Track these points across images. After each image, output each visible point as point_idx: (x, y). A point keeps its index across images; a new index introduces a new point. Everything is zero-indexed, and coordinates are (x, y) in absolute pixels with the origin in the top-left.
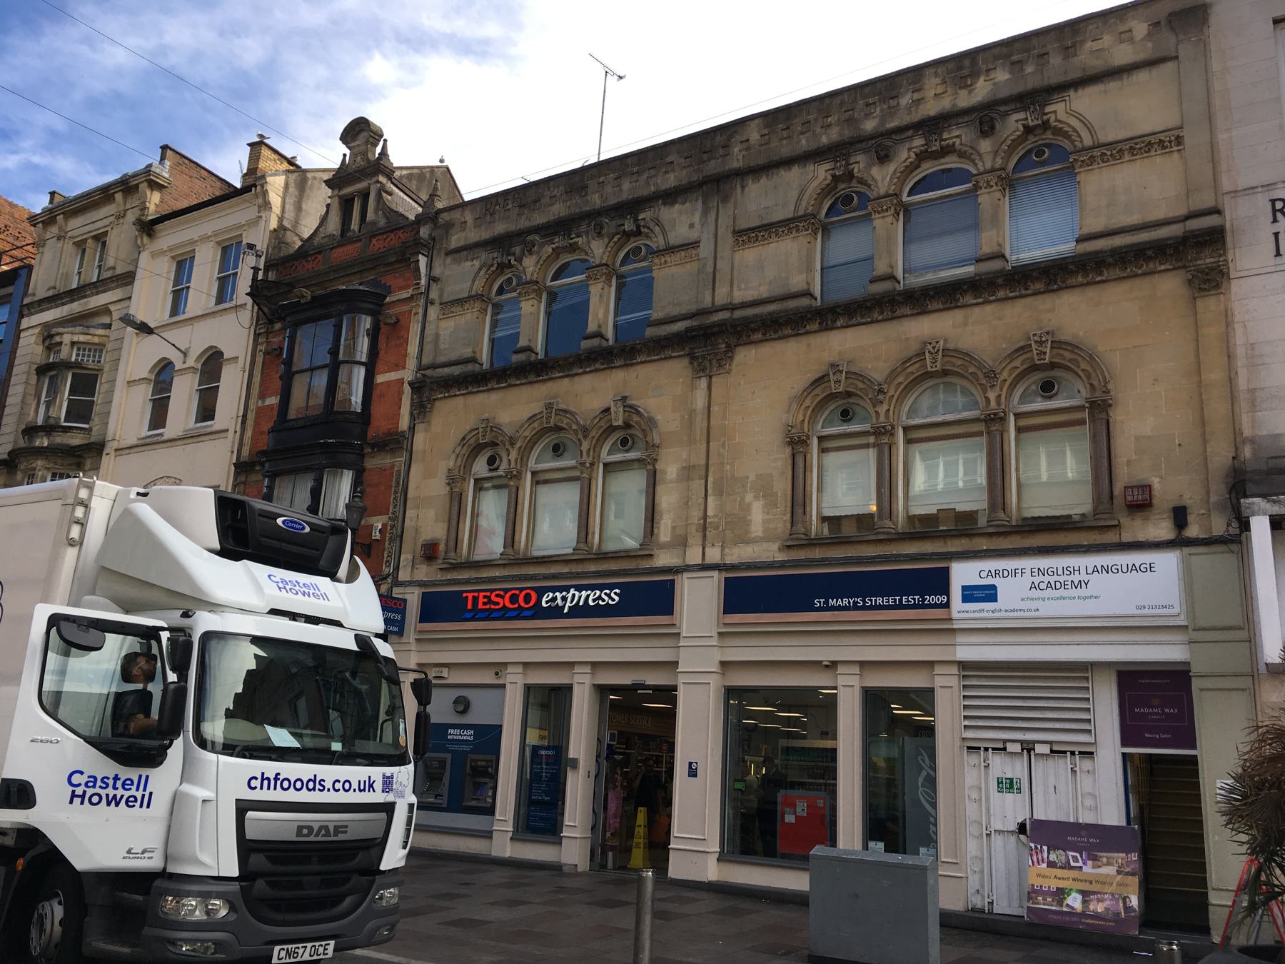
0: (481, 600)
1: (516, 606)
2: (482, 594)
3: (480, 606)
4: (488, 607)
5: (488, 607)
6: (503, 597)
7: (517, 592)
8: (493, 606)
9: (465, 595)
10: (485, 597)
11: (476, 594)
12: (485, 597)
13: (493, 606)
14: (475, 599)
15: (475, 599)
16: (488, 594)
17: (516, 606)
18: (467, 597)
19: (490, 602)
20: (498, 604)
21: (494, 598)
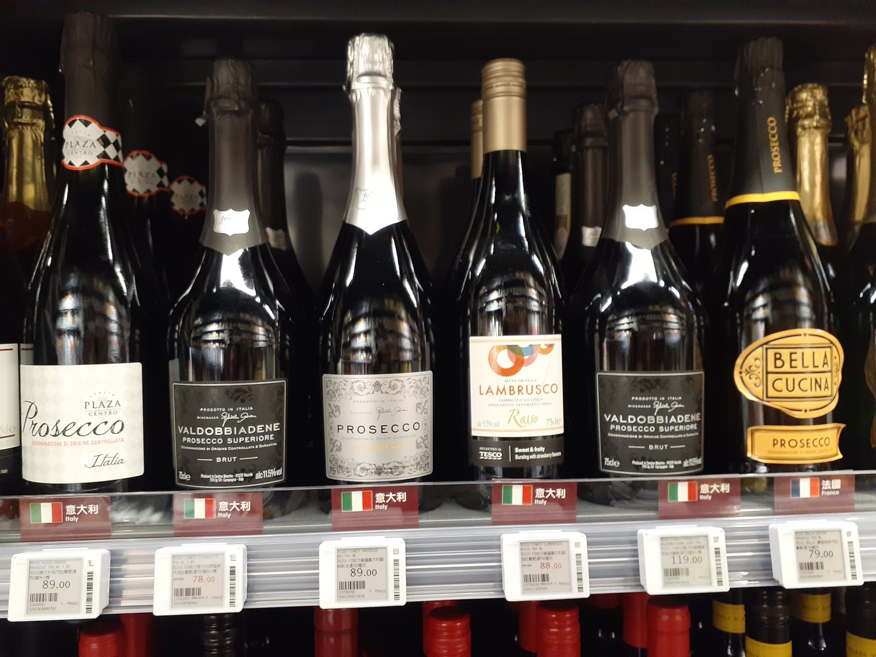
0: (485, 455)
2: (485, 453)
14: (483, 454)
15: (483, 454)
18: (480, 454)
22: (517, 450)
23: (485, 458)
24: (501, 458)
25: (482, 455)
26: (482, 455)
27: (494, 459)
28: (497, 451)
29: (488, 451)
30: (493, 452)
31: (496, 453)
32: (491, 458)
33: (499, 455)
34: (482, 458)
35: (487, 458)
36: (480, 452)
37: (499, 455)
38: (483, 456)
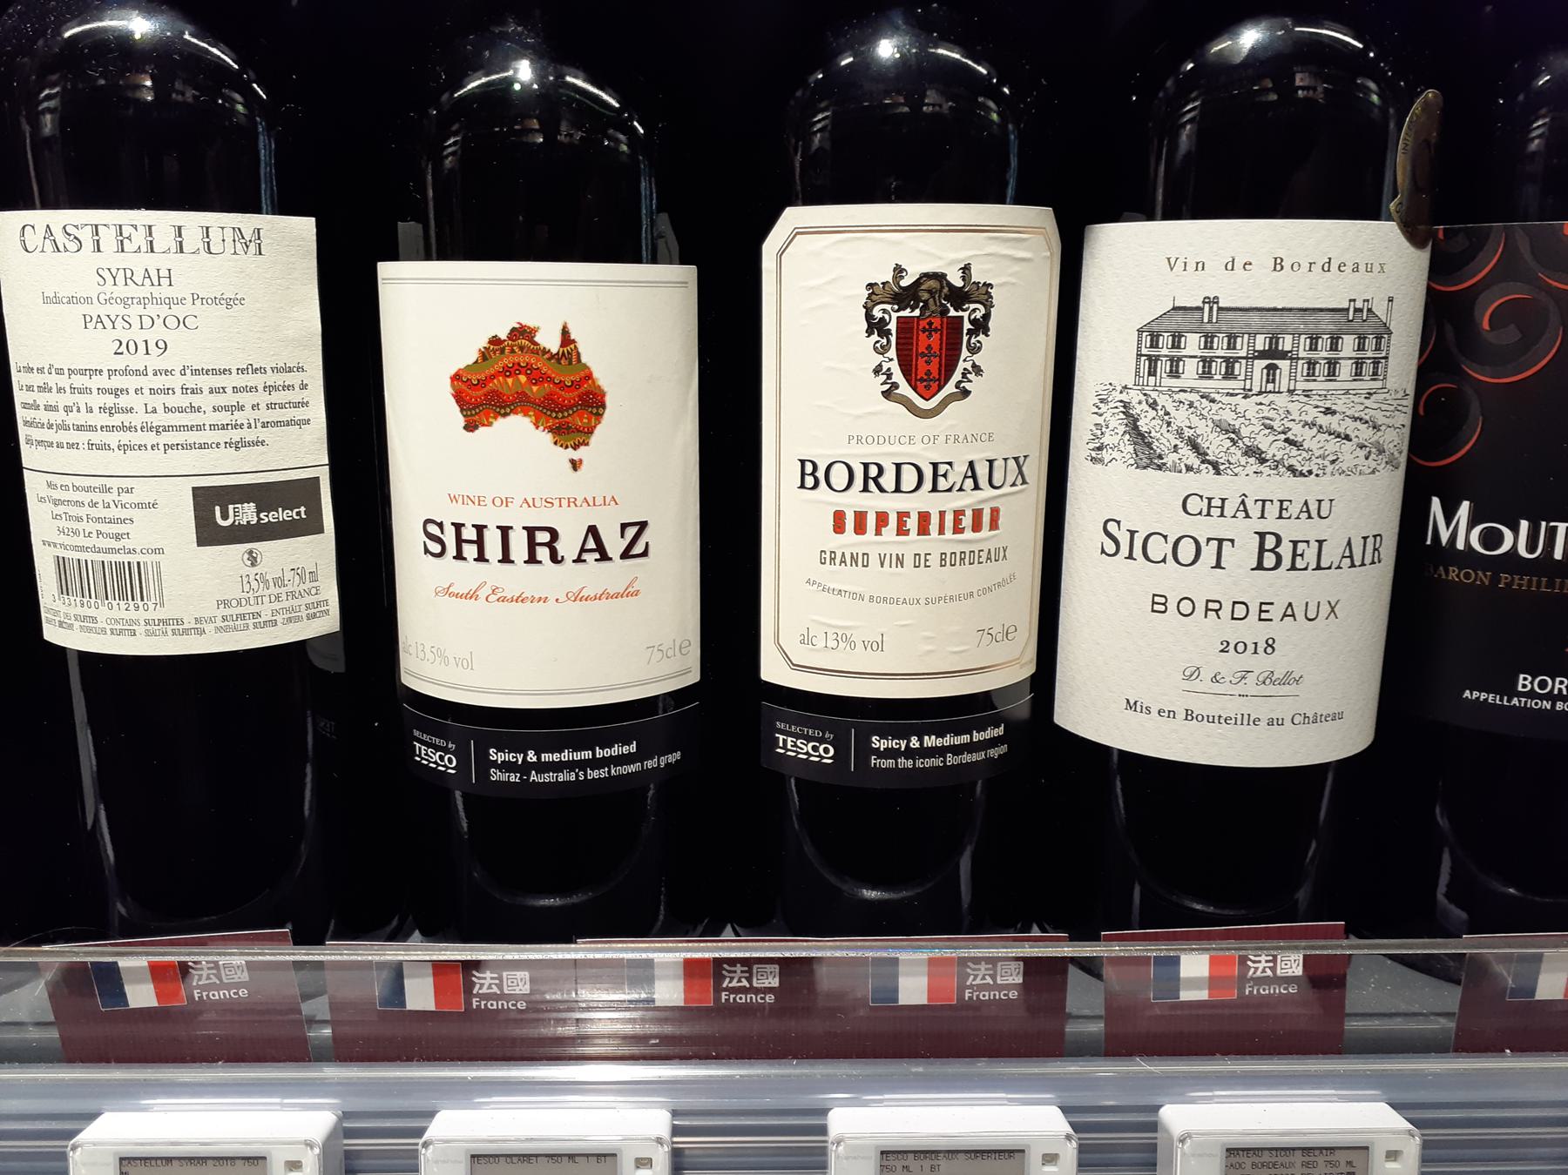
0: (789, 744)
1: (817, 754)
2: (789, 739)
3: (789, 747)
4: (795, 749)
5: (795, 749)
6: (806, 745)
7: (818, 744)
8: (799, 750)
9: (777, 735)
10: (792, 741)
11: (785, 737)
12: (792, 741)
13: (799, 750)
15: (785, 741)
16: (795, 740)
17: (817, 754)
19: (795, 745)
20: (802, 749)
21: (798, 743)
22: (878, 743)
23: (789, 753)
24: (830, 761)
25: (781, 745)
26: (781, 745)
27: (812, 759)
28: (822, 741)
29: (797, 736)
30: (809, 739)
31: (818, 744)
32: (805, 757)
33: (826, 750)
34: (782, 751)
35: (794, 754)
36: (777, 735)
37: (826, 750)
38: (785, 747)
